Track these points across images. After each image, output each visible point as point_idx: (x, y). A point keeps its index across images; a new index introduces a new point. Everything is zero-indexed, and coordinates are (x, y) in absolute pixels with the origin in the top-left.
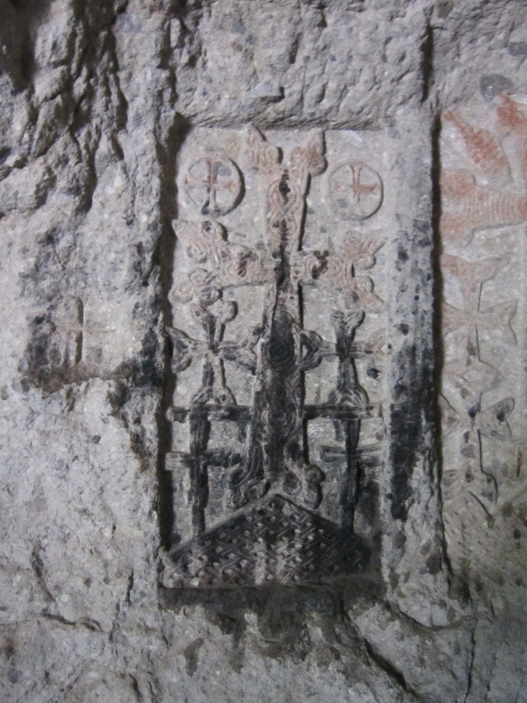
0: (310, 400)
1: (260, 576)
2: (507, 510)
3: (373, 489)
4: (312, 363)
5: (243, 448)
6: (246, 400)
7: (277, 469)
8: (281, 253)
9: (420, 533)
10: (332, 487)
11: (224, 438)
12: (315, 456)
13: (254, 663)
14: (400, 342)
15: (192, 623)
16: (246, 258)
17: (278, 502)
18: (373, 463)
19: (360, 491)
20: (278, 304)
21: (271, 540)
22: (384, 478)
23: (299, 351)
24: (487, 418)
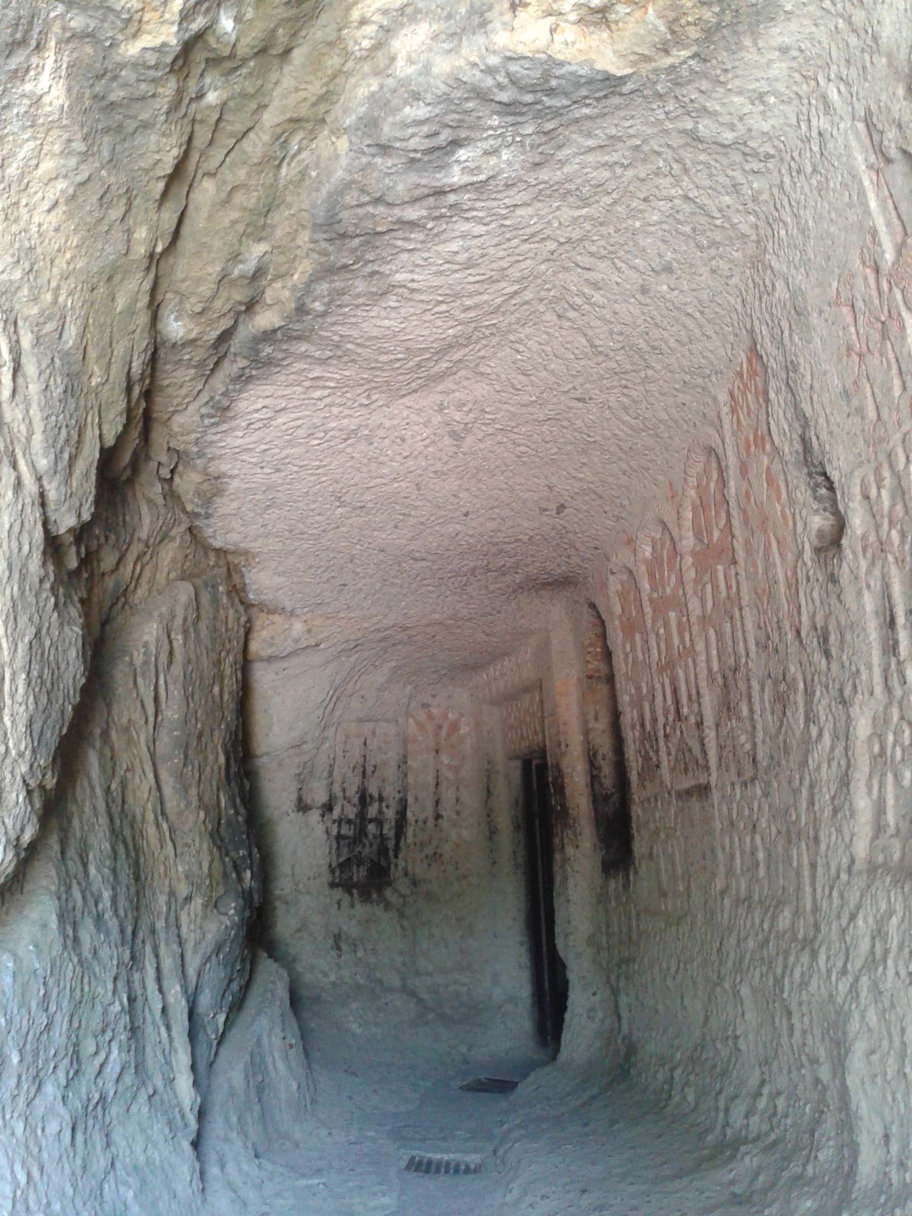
0: (369, 817)
1: (355, 879)
2: (427, 857)
3: (387, 849)
4: (371, 804)
5: (351, 833)
6: (352, 816)
7: (361, 841)
8: (364, 766)
9: (401, 864)
10: (375, 847)
11: (346, 830)
12: (371, 837)
13: (358, 906)
14: (398, 796)
15: (338, 893)
16: (354, 768)
17: (360, 853)
18: (388, 838)
19: (383, 851)
20: (363, 783)
21: (358, 866)
22: (391, 844)
23: (368, 800)
24: (420, 823)
